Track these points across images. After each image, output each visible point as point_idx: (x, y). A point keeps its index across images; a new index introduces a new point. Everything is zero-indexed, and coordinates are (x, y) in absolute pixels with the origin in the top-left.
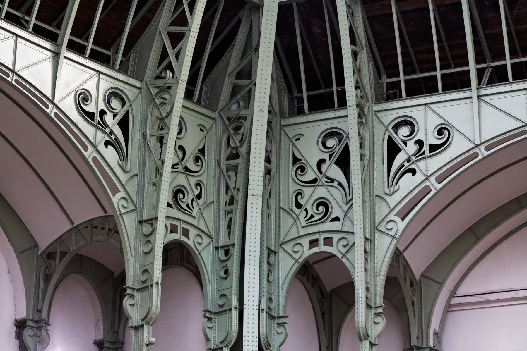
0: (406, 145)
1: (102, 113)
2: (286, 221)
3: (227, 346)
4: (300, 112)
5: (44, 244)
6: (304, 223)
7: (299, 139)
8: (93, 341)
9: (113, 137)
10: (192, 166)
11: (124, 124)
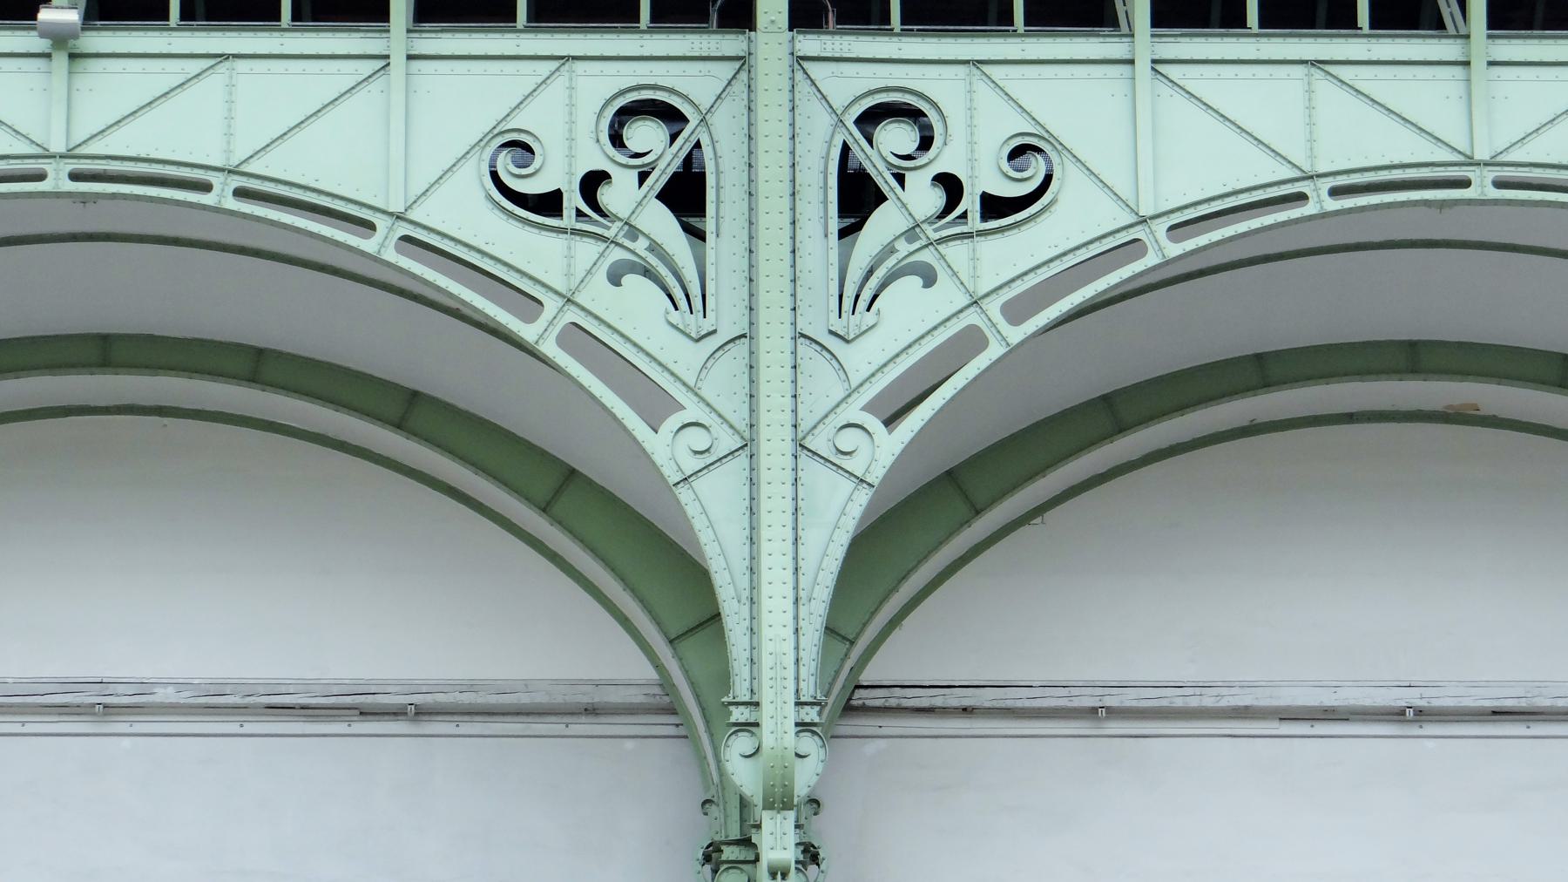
0: (903, 187)
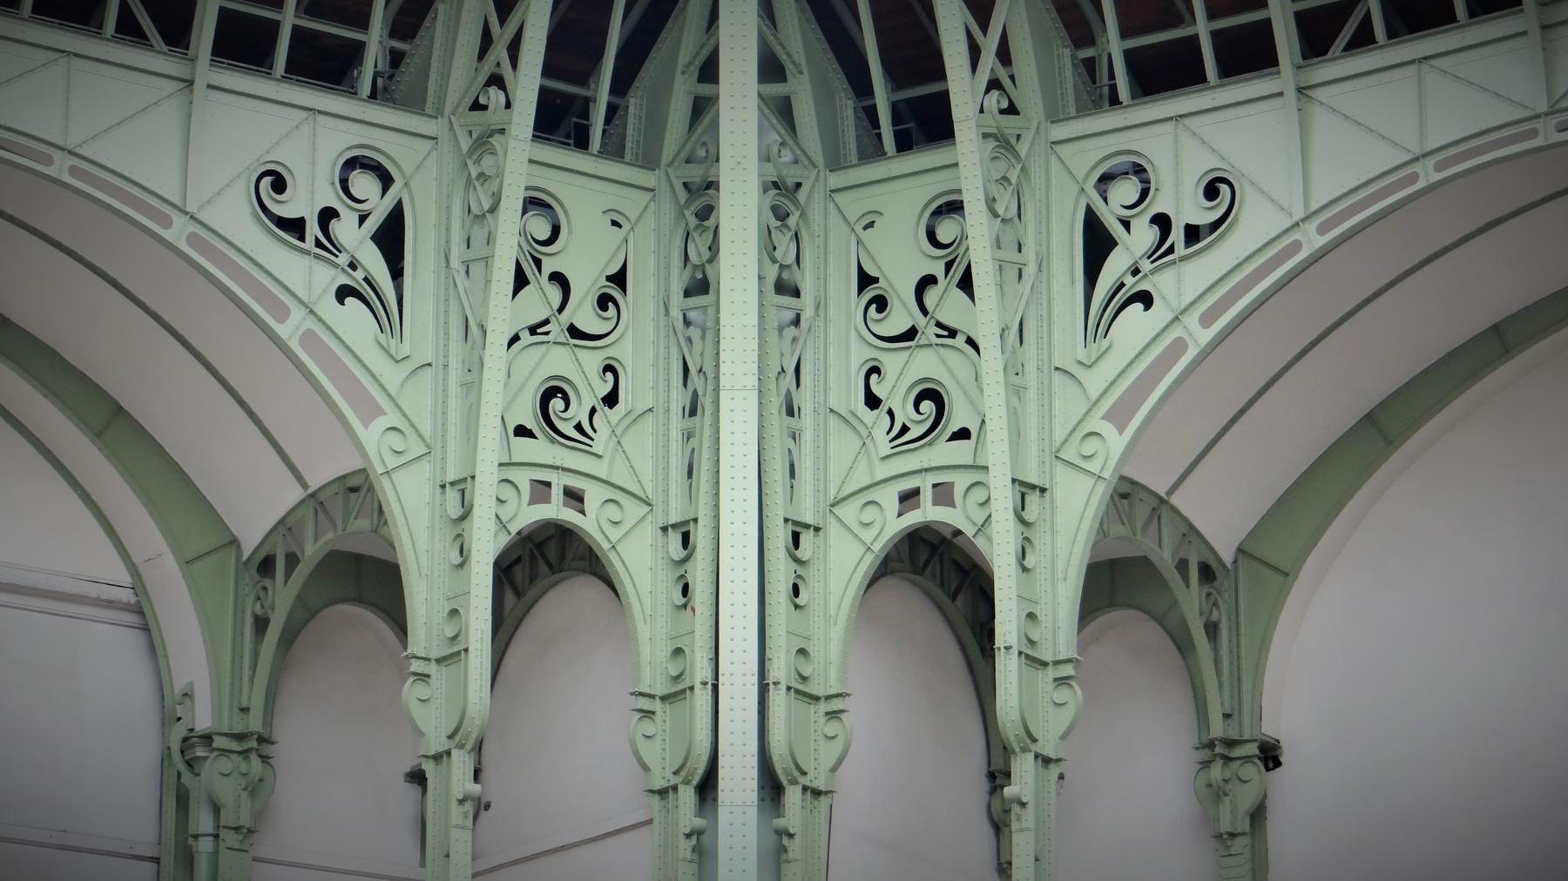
1: (327, 216)
2: (842, 444)
3: (687, 782)
4: (871, 151)
5: (251, 537)
6: (885, 447)
7: (871, 225)
8: (408, 769)
9: (359, 274)
10: (589, 320)
11: (391, 238)
